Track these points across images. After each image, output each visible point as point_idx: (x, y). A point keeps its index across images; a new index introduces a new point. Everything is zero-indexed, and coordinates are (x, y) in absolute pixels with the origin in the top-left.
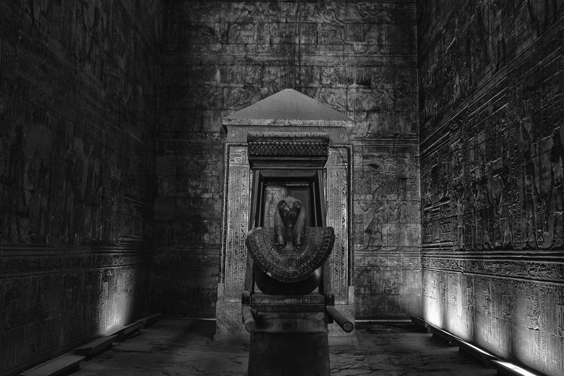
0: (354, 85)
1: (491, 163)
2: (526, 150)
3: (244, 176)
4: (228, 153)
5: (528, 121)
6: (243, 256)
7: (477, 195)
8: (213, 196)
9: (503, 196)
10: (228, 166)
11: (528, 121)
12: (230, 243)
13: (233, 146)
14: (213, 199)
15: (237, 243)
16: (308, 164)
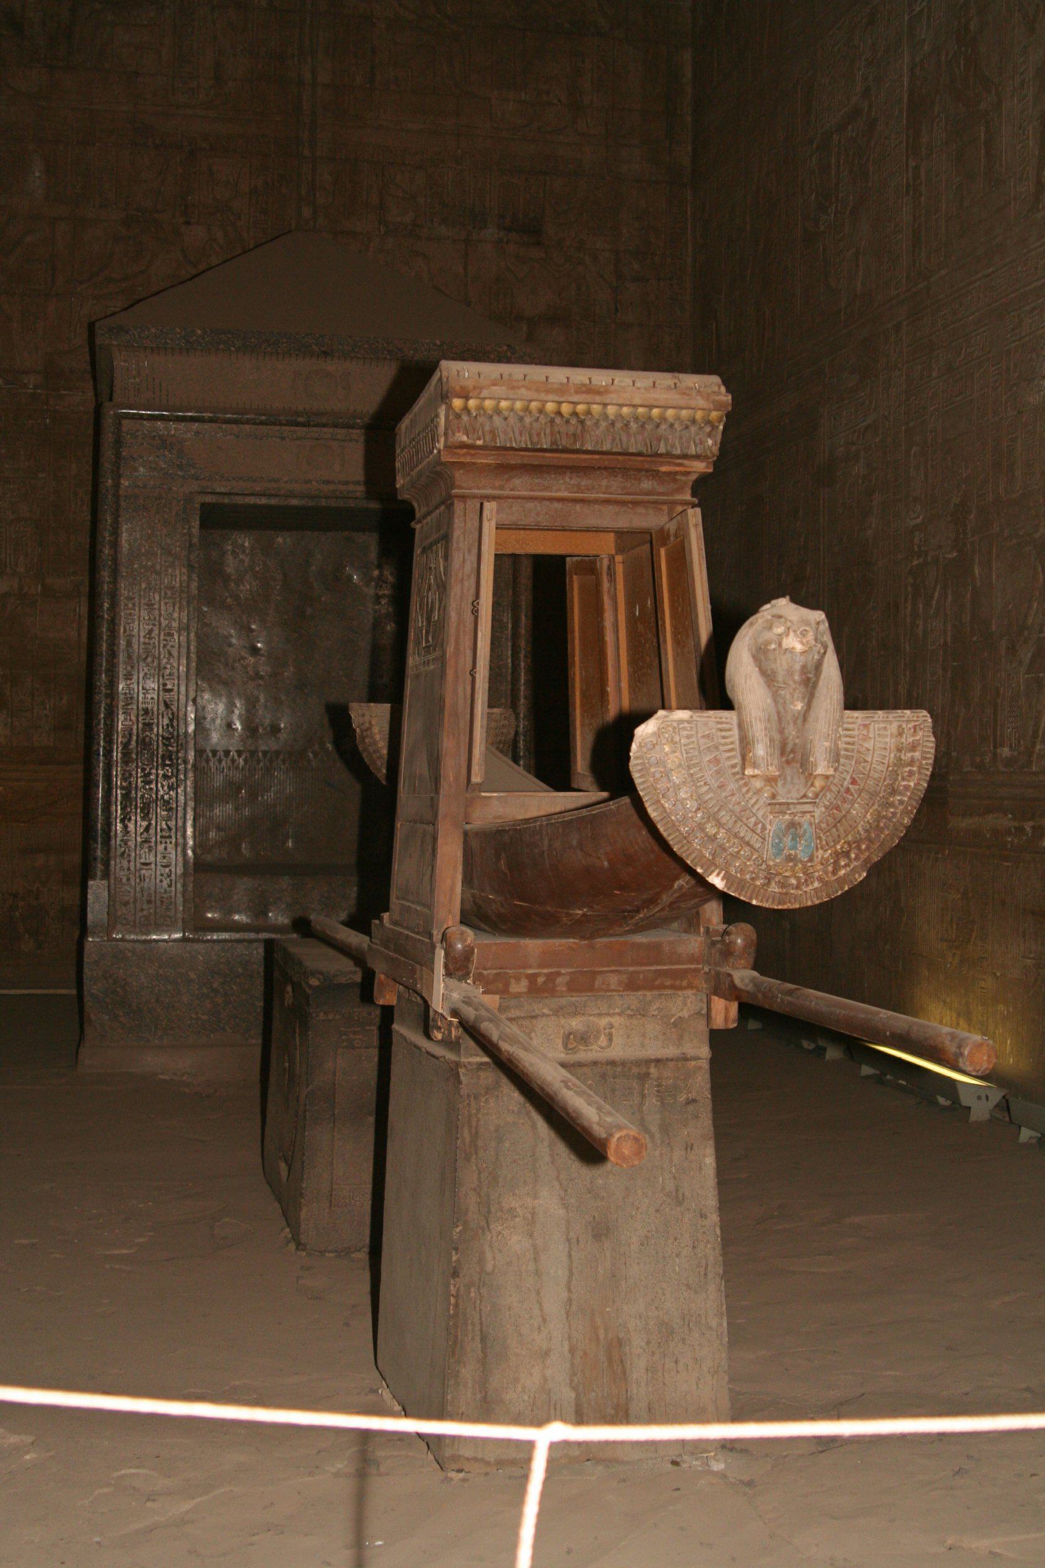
0: (491, 233)
6: (171, 788)
10: (117, 485)
12: (126, 746)
16: (647, 484)
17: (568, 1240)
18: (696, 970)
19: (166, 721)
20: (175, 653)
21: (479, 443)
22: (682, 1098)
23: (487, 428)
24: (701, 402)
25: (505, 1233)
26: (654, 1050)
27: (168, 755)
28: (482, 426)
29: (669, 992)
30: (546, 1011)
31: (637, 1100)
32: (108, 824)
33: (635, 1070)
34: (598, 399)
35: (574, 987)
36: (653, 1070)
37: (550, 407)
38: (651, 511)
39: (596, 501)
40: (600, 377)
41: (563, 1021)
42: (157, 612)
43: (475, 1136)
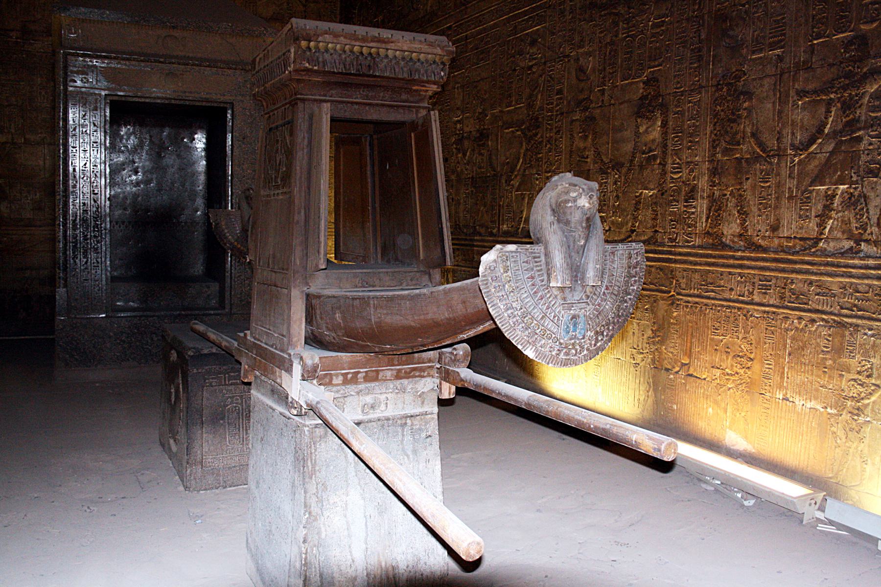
1: (501, 111)
2: (581, 97)
3: (96, 109)
4: (66, 67)
5: (589, 54)
6: (98, 242)
7: (464, 155)
8: (13, 139)
9: (524, 160)
10: (66, 89)
11: (589, 54)
12: (74, 221)
13: (73, 54)
14: (13, 143)
15: (84, 221)
16: (404, 97)
17: (365, 517)
18: (432, 367)
19: (95, 209)
20: (98, 175)
21: (316, 68)
22: (423, 435)
23: (321, 59)
24: (439, 51)
25: (331, 516)
26: (410, 411)
27: (96, 226)
28: (318, 58)
29: (418, 379)
30: (352, 393)
31: (400, 437)
32: (66, 260)
33: (399, 422)
34: (383, 46)
35: (367, 379)
36: (409, 421)
37: (356, 49)
38: (407, 112)
39: (377, 105)
40: (386, 33)
41: (361, 398)
42: (88, 155)
43: (314, 466)
